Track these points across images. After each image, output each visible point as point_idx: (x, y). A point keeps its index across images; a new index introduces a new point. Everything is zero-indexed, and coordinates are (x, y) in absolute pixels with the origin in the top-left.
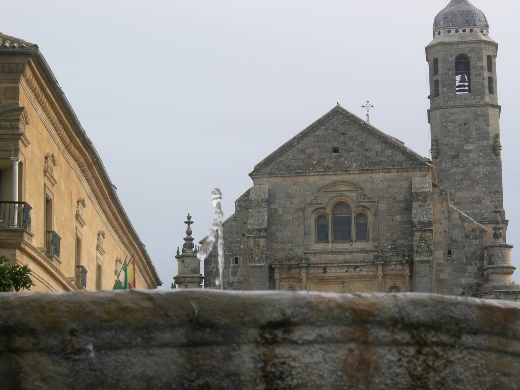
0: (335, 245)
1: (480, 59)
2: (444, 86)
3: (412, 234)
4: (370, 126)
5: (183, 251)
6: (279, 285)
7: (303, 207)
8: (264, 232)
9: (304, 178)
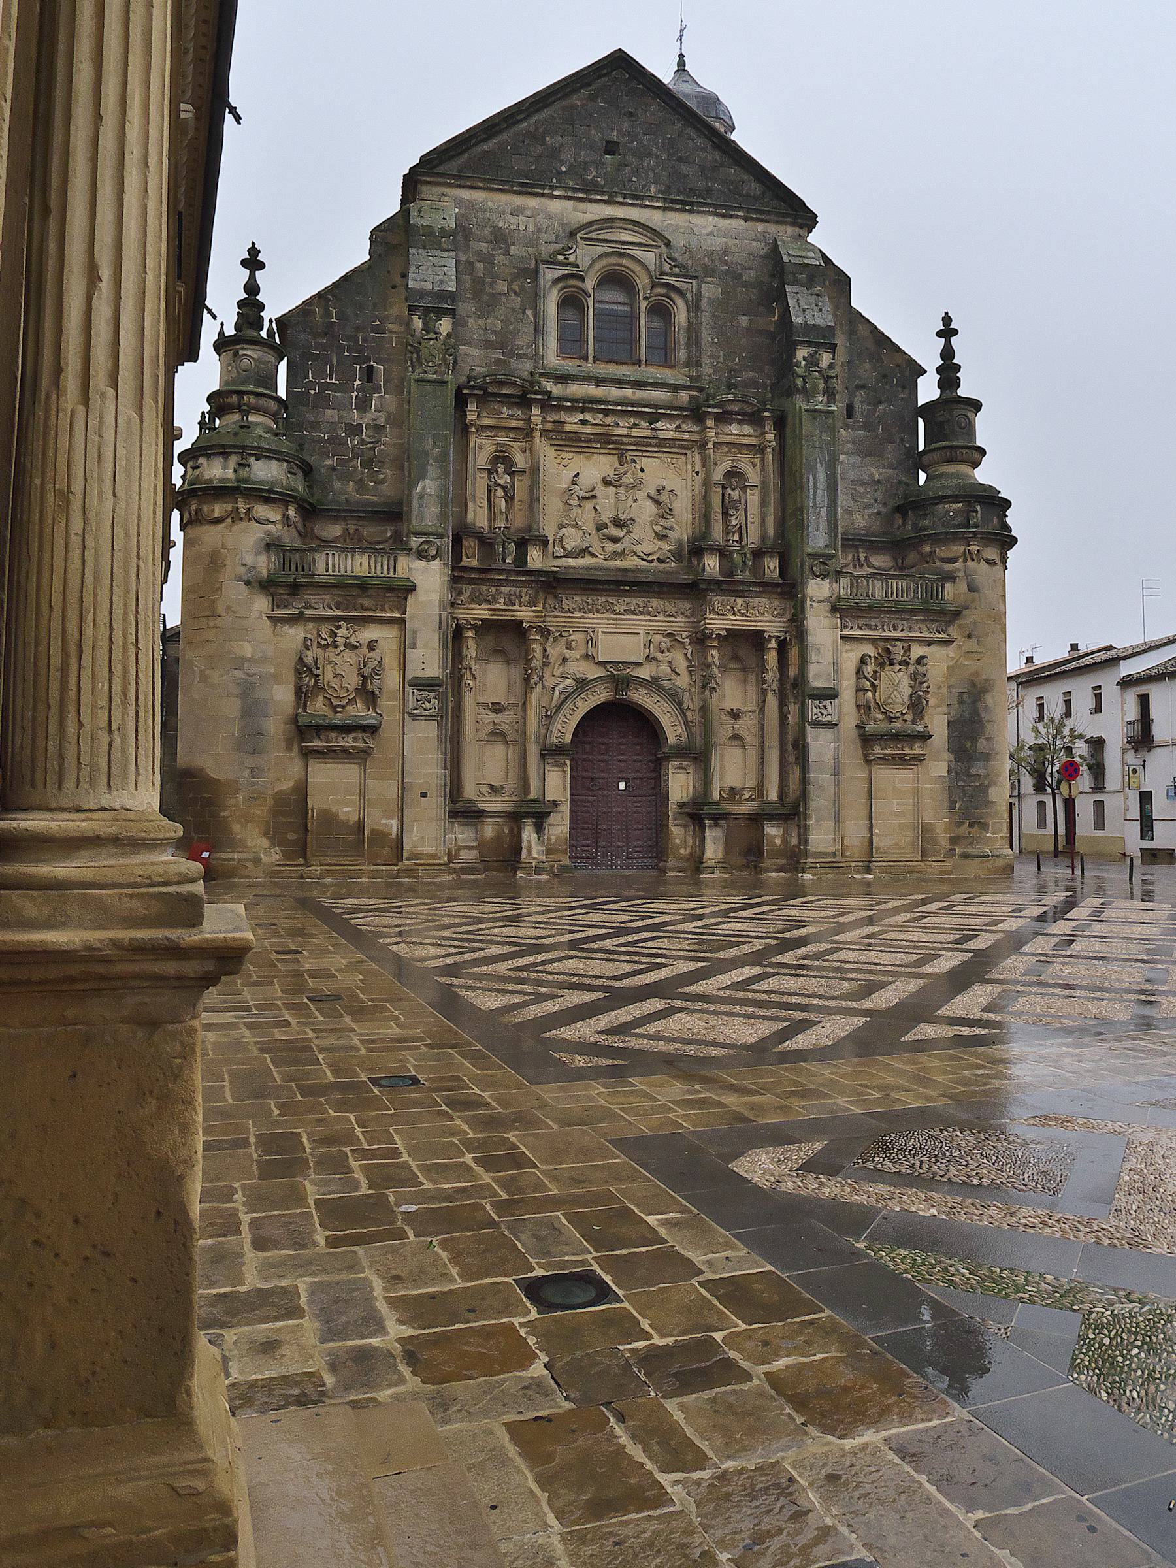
0: (601, 365)
7: (533, 266)
9: (538, 200)
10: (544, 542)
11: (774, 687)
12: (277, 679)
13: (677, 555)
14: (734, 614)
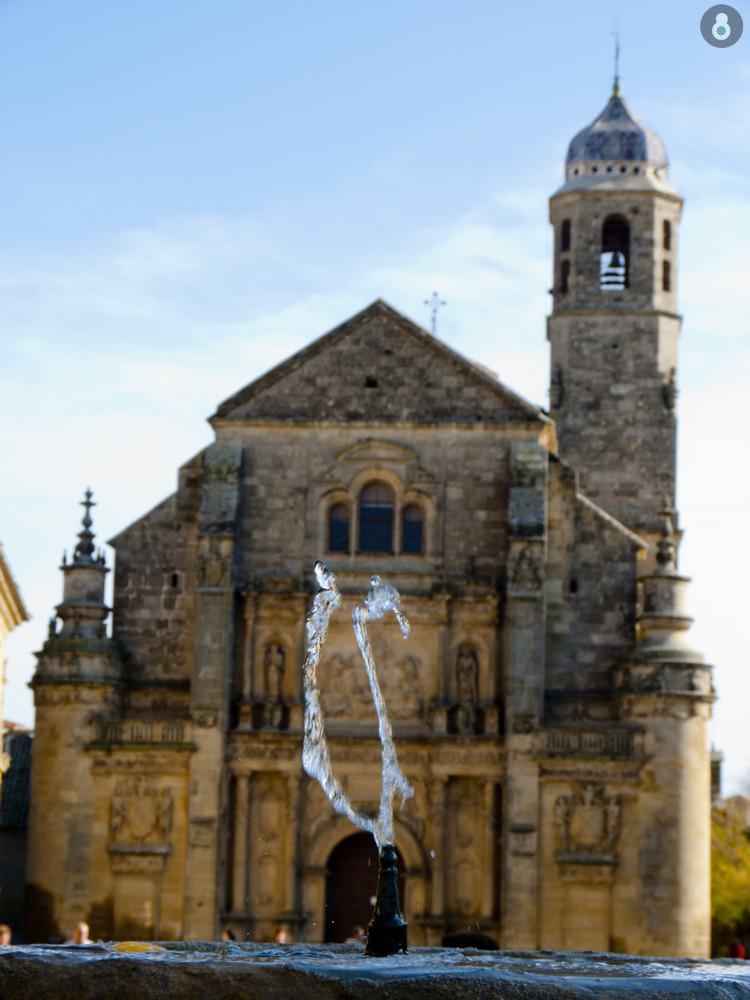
1: (649, 225)
2: (580, 272)
3: (507, 547)
4: (438, 342)
5: (75, 558)
8: (229, 529)
12: (95, 817)
13: (420, 713)
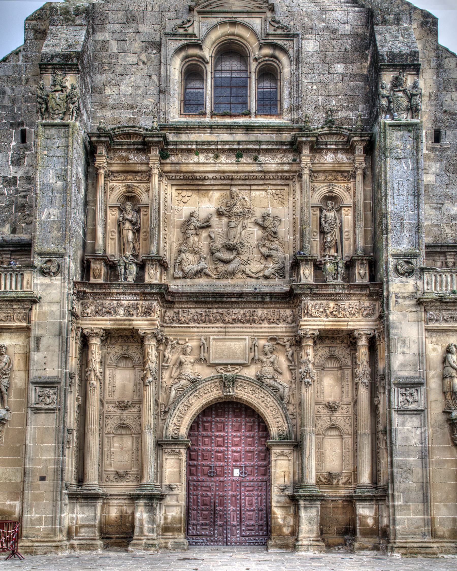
6: (106, 185)
10: (163, 266)
11: (366, 380)
14: (327, 316)
